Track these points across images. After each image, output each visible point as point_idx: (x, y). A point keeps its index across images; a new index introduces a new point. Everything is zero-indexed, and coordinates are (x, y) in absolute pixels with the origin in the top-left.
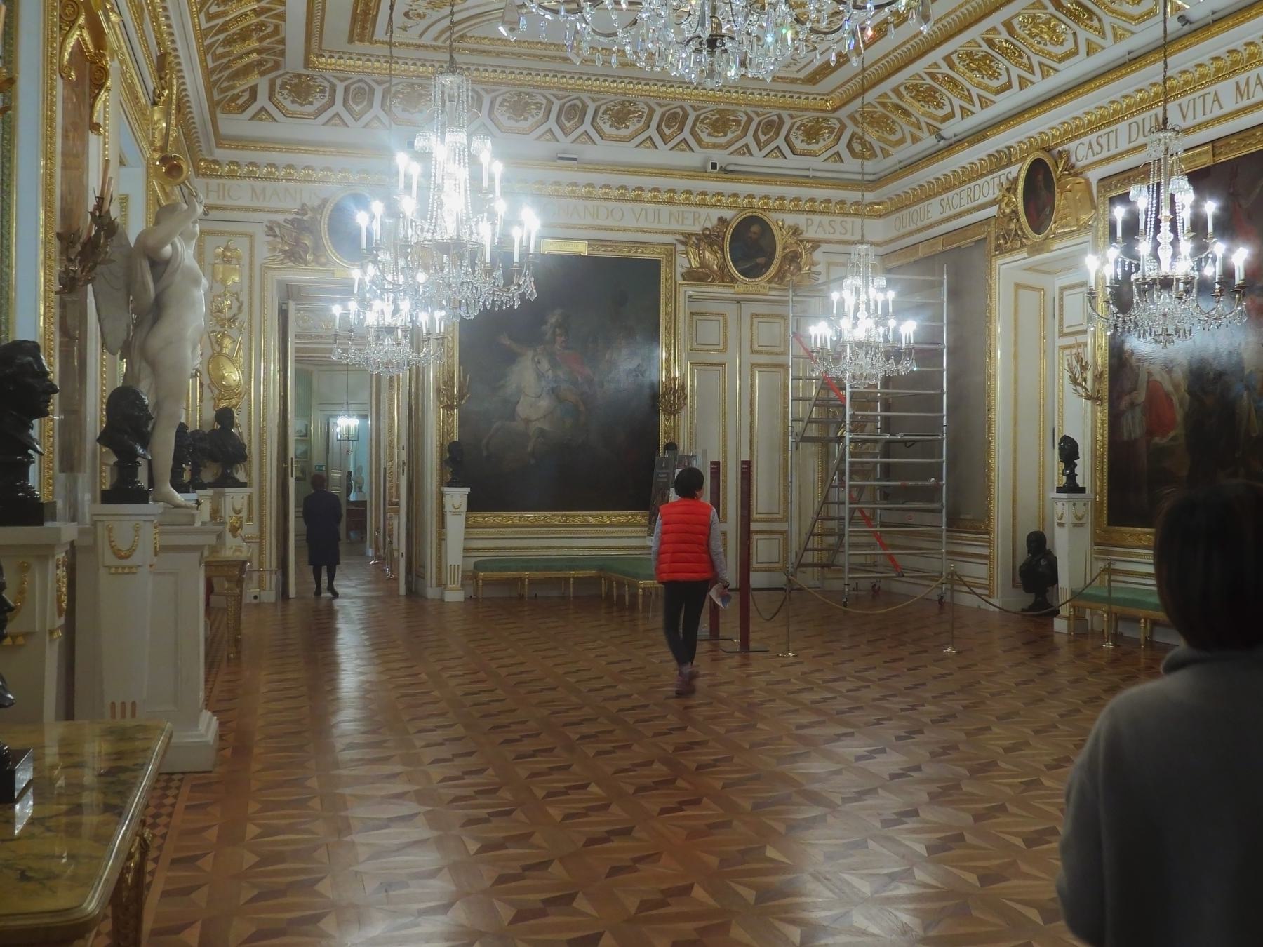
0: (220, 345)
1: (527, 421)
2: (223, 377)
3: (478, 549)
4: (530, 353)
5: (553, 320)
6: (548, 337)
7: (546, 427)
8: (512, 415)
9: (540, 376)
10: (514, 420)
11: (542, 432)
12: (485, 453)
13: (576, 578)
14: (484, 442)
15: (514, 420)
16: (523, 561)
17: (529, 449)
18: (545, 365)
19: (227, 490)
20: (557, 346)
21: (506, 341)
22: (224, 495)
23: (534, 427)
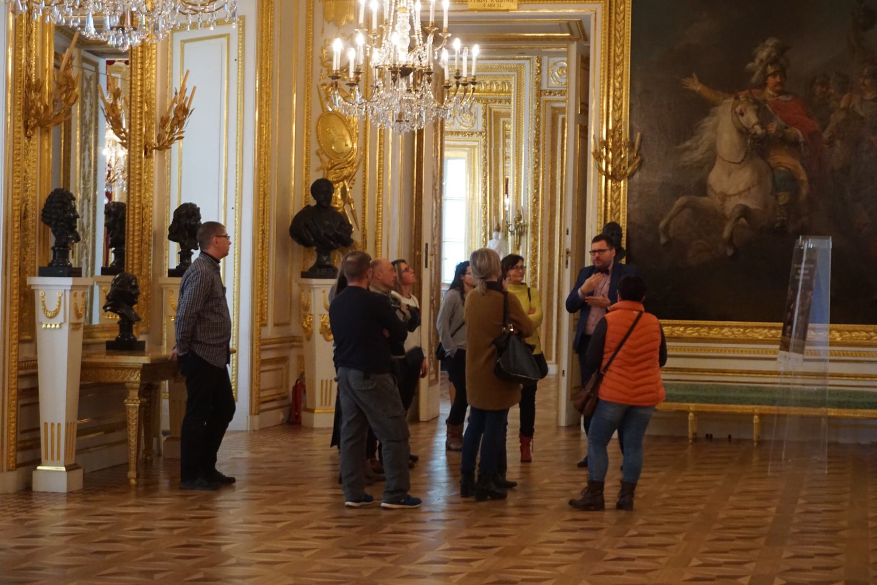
0: (328, 98)
1: (724, 197)
2: (333, 142)
3: (733, 372)
4: (731, 100)
5: (763, 54)
6: (754, 79)
7: (751, 204)
8: (703, 188)
9: (743, 132)
10: (705, 194)
11: (745, 212)
12: (663, 240)
13: (697, 413)
14: (662, 224)
15: (705, 194)
16: (751, 390)
17: (726, 234)
18: (751, 118)
19: (315, 281)
20: (769, 91)
21: (696, 86)
22: (310, 288)
23: (731, 206)
